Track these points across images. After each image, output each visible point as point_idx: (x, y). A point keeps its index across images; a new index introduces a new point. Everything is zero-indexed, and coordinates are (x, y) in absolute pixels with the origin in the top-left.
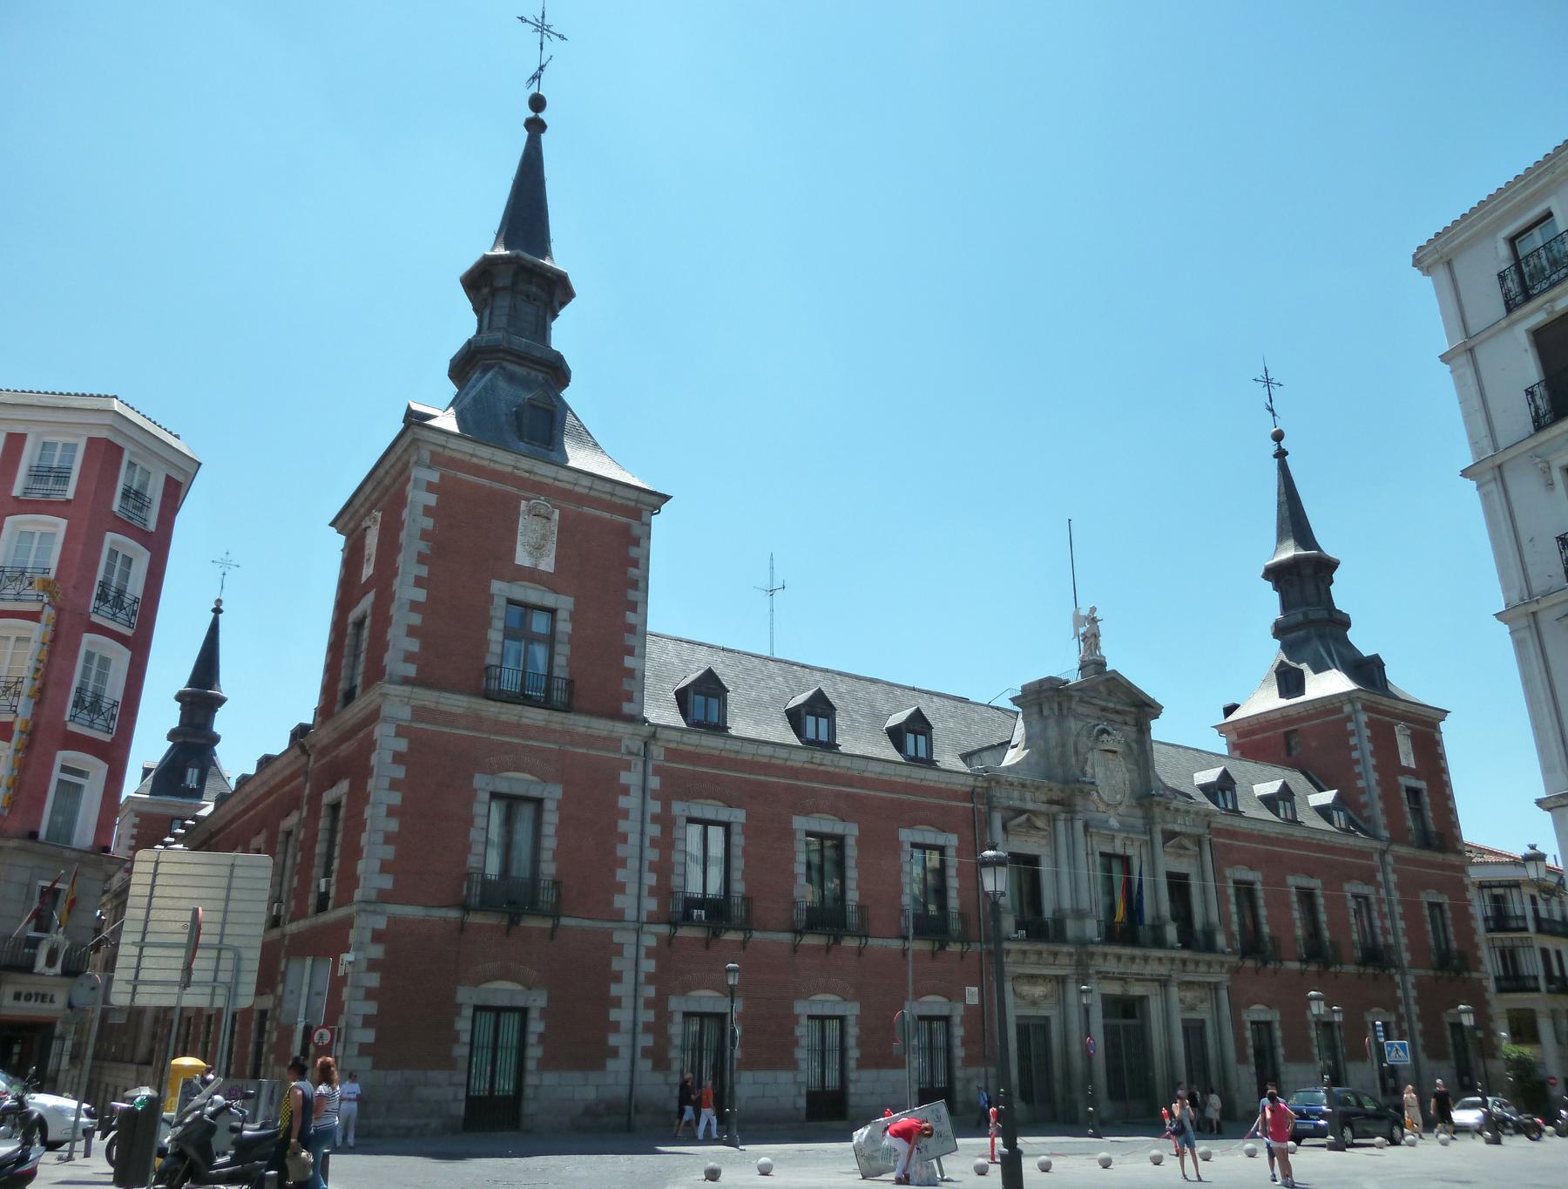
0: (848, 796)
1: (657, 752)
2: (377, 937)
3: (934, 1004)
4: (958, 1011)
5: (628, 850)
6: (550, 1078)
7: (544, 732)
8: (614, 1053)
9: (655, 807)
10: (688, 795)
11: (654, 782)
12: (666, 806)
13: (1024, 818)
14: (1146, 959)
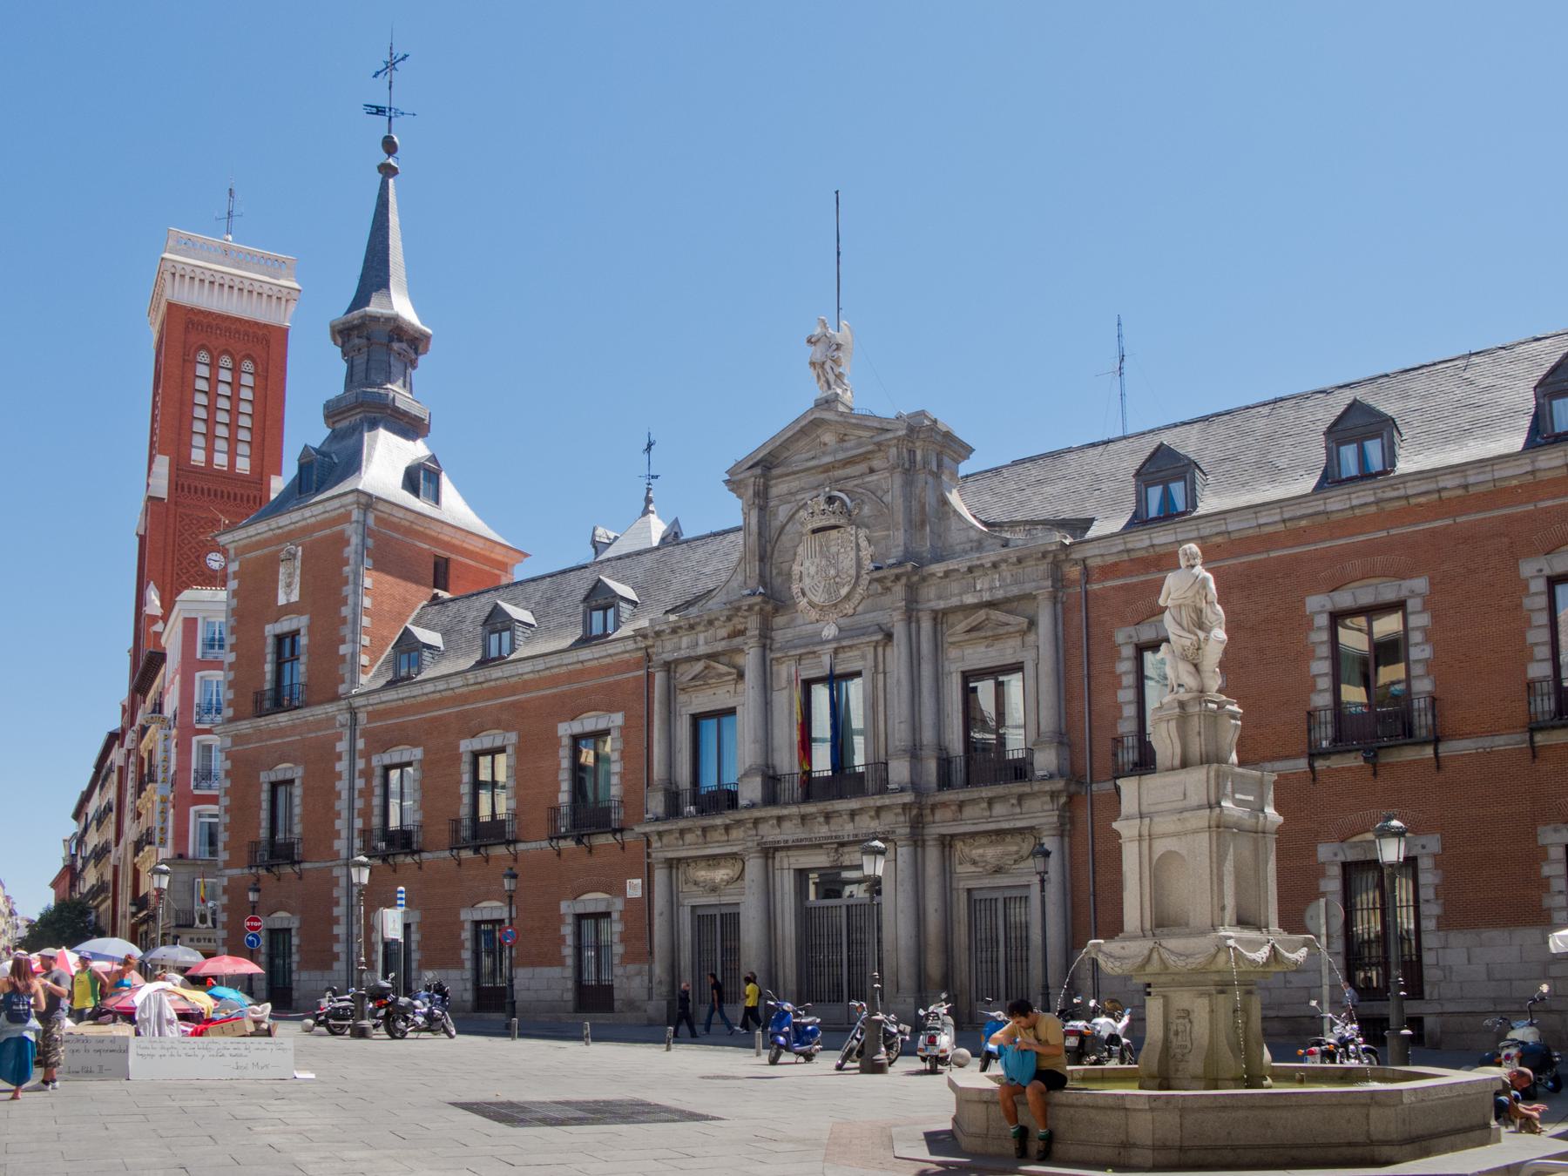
0: (513, 704)
1: (362, 717)
2: (225, 890)
3: (594, 901)
4: (618, 905)
5: (342, 805)
6: (304, 975)
7: (293, 728)
8: (336, 957)
9: (361, 764)
10: (386, 747)
11: (360, 744)
12: (369, 761)
13: (699, 666)
14: (828, 817)
